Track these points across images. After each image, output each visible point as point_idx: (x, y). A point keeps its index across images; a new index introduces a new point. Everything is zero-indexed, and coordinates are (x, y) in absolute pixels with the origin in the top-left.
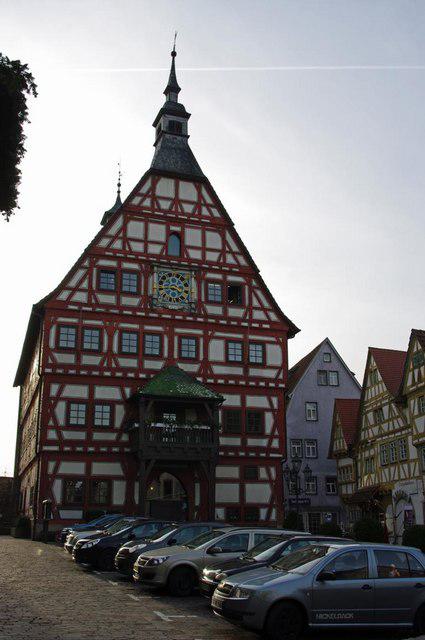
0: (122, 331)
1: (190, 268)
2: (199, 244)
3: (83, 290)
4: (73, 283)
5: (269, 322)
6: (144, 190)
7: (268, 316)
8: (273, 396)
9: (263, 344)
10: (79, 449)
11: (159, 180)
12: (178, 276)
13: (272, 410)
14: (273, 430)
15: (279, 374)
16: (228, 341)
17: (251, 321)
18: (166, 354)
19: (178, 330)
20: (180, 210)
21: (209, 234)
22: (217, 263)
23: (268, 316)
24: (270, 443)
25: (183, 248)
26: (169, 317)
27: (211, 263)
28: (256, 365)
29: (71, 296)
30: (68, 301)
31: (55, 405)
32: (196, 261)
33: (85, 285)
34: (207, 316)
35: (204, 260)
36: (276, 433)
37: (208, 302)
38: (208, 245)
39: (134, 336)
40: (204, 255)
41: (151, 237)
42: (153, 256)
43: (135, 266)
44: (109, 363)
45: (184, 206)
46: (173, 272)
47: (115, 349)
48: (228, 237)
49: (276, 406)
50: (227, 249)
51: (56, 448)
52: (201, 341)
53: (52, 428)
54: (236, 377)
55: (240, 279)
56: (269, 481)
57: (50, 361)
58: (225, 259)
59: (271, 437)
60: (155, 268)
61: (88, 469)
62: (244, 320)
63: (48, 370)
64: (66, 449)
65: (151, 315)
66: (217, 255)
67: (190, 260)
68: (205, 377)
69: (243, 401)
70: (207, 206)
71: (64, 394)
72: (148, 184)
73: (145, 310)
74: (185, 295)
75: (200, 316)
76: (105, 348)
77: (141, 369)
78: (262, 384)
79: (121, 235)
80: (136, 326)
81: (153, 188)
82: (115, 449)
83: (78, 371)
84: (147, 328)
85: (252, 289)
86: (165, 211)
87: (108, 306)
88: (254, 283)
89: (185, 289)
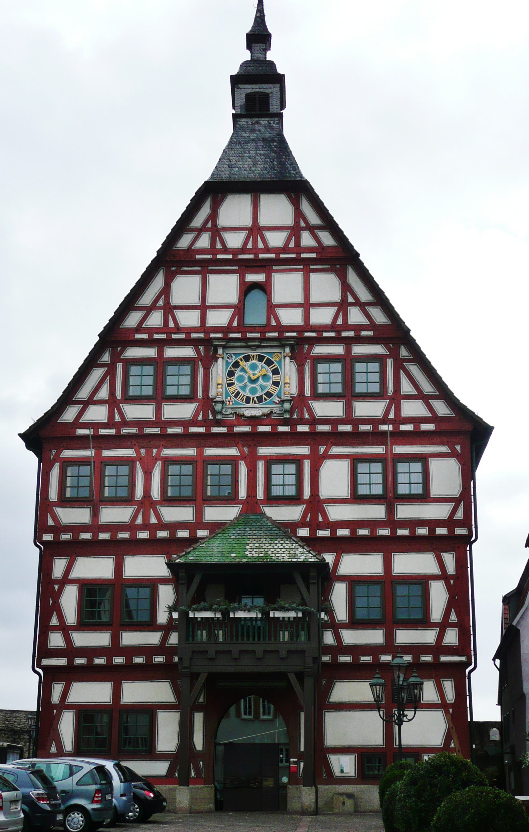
0: (168, 462)
1: (281, 342)
2: (300, 299)
3: (101, 402)
4: (83, 393)
5: (434, 418)
6: (198, 221)
7: (430, 408)
8: (447, 551)
9: (423, 459)
10: (100, 661)
12: (261, 358)
13: (444, 576)
16: (355, 460)
17: (399, 420)
18: (243, 494)
19: (263, 451)
20: (261, 245)
21: (315, 278)
22: (332, 327)
23: (430, 408)
24: (441, 636)
25: (271, 308)
26: (247, 429)
27: (320, 329)
28: (410, 499)
29: (81, 414)
30: (77, 423)
31: (61, 590)
32: (291, 328)
33: (104, 393)
34: (314, 421)
35: (307, 326)
37: (317, 396)
38: (314, 299)
39: (187, 469)
42: (216, 330)
43: (187, 352)
44: (146, 517)
46: (250, 352)
47: (156, 494)
48: (353, 279)
50: (350, 299)
51: (62, 662)
52: (307, 465)
53: (55, 629)
54: (372, 524)
55: (378, 349)
56: (443, 705)
57: (51, 522)
59: (443, 626)
60: (220, 351)
61: (117, 693)
63: (48, 537)
64: (79, 661)
65: (215, 430)
66: (332, 311)
68: (314, 526)
70: (312, 229)
71: (75, 574)
72: (205, 210)
73: (206, 423)
74: (275, 391)
75: (303, 422)
76: (139, 493)
77: (199, 523)
78: (422, 531)
79: (161, 303)
80: (191, 452)
81: (214, 215)
82: (159, 659)
83: (57, 536)
84: (210, 452)
85: (399, 366)
86: (235, 252)
87: (141, 424)
88: (404, 353)
89: (273, 378)
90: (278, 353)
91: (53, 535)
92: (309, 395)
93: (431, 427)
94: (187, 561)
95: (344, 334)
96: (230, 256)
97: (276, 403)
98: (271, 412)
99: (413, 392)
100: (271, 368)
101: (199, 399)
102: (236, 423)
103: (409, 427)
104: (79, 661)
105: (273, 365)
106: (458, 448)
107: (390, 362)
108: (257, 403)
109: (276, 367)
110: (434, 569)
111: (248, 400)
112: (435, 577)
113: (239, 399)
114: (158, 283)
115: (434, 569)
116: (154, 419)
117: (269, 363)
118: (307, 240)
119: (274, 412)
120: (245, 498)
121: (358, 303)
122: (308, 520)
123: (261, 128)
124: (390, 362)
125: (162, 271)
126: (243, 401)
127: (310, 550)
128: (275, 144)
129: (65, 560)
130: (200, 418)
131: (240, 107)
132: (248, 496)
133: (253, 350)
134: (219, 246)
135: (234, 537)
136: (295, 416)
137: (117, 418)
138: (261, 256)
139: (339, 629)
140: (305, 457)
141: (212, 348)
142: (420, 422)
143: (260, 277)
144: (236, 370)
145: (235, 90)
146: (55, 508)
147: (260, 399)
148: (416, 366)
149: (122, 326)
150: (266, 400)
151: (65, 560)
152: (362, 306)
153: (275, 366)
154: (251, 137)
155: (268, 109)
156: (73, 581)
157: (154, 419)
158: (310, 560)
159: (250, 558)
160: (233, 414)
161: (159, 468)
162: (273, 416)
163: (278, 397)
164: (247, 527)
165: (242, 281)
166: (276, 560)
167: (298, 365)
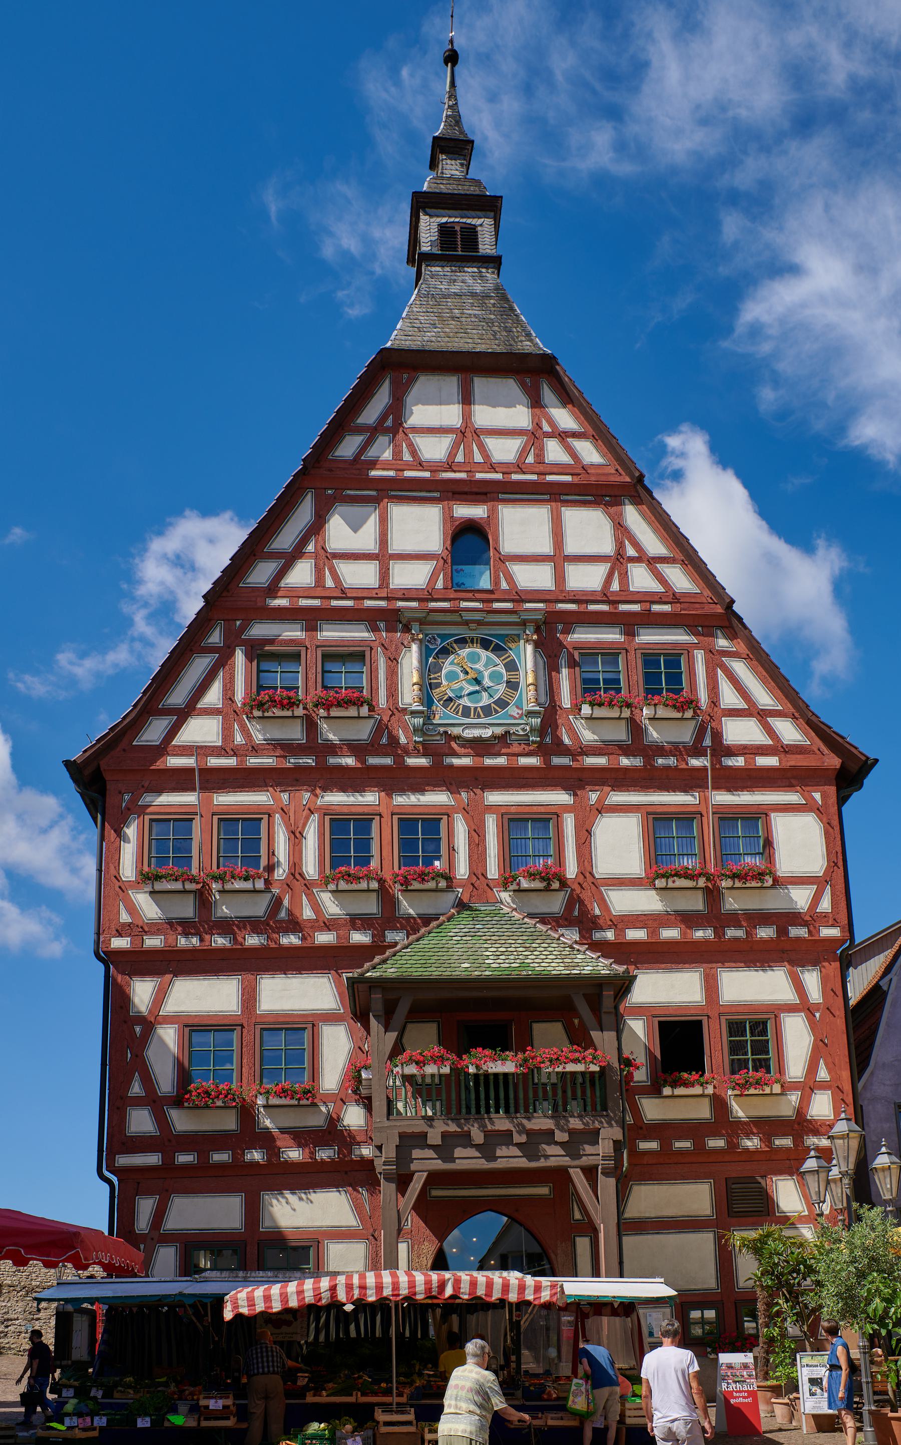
2: (547, 548)
4: (178, 697)
5: (778, 748)
6: (370, 414)
7: (770, 731)
10: (220, 1157)
11: (411, 382)
13: (804, 1006)
14: (812, 1068)
15: (817, 899)
17: (721, 750)
19: (495, 798)
20: (478, 458)
22: (604, 596)
23: (770, 731)
35: (561, 593)
36: (823, 1074)
38: (571, 548)
40: (560, 577)
41: (397, 545)
42: (406, 595)
45: (491, 443)
49: (815, 993)
50: (631, 552)
52: (569, 822)
55: (680, 637)
58: (624, 578)
59: (809, 1086)
62: (697, 750)
66: (601, 570)
67: (520, 597)
69: (711, 987)
71: (171, 1006)
78: (765, 933)
79: (311, 548)
85: (715, 660)
86: (435, 467)
90: (514, 635)
91: (129, 939)
92: (569, 706)
93: (771, 761)
94: (384, 974)
95: (623, 607)
96: (427, 474)
97: (515, 718)
98: (507, 732)
99: (743, 705)
100: (503, 660)
101: (383, 709)
102: (447, 751)
103: (739, 762)
104: (183, 1158)
105: (507, 655)
106: (817, 796)
107: (699, 656)
108: (483, 716)
109: (511, 658)
110: (788, 995)
111: (466, 712)
112: (791, 1009)
113: (452, 711)
114: (304, 513)
115: (788, 995)
116: (304, 741)
117: (498, 650)
118: (554, 452)
119: (511, 732)
120: (466, 877)
121: (642, 558)
122: (576, 914)
123: (467, 278)
124: (699, 656)
125: (310, 494)
126: (457, 713)
127: (599, 957)
128: (492, 301)
129: (153, 984)
130: (384, 741)
131: (429, 244)
132: (473, 873)
133: (471, 630)
134: (407, 457)
135: (459, 938)
136: (548, 740)
137: (239, 739)
138: (479, 476)
139: (636, 1097)
140: (566, 808)
141: (401, 625)
142: (754, 754)
143: (476, 512)
144: (444, 663)
145: (421, 217)
146: (133, 893)
147: (487, 711)
148: (742, 664)
149: (243, 583)
150: (497, 712)
151: (153, 984)
152: (652, 562)
153: (509, 657)
154: (453, 291)
155: (476, 249)
156: (170, 1020)
157: (304, 741)
158: (602, 972)
159: (495, 969)
160: (442, 735)
161: (315, 828)
162: (510, 740)
163: (517, 707)
164: (477, 923)
165: (448, 517)
166: (542, 972)
167: (549, 657)
